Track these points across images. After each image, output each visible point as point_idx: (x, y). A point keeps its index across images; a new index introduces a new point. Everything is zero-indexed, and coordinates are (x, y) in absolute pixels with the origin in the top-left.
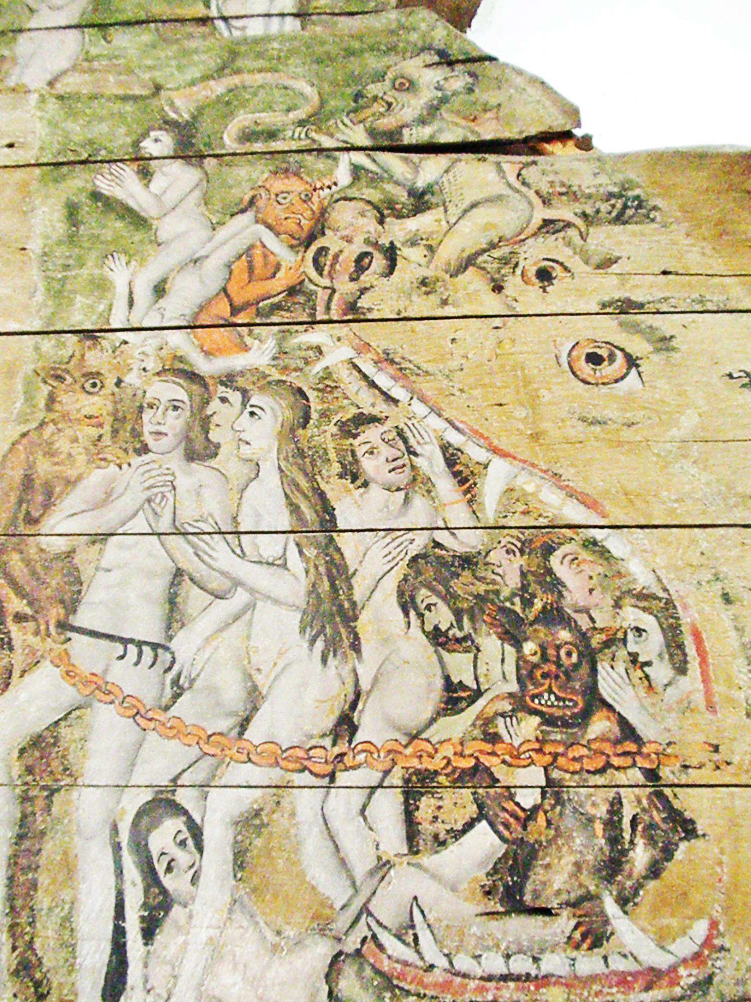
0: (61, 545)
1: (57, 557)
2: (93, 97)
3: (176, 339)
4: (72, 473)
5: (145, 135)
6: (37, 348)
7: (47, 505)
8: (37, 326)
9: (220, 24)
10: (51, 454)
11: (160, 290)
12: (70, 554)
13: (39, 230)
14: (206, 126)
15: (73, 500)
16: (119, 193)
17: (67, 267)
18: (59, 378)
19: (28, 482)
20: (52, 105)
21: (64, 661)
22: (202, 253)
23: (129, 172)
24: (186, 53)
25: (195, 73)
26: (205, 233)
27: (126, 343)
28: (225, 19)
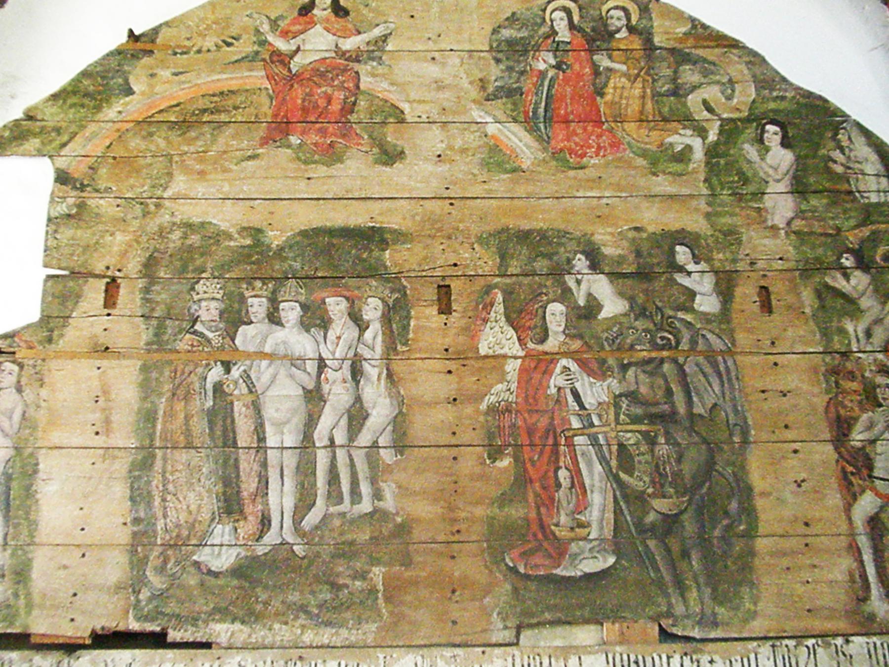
0: (859, 444)
1: (860, 449)
2: (811, 233)
3: (880, 356)
4: (854, 415)
5: (840, 257)
6: (824, 361)
7: (850, 428)
8: (821, 350)
9: (857, 194)
10: (845, 407)
11: (868, 334)
12: (864, 448)
13: (807, 303)
14: (867, 253)
15: (859, 427)
16: (837, 285)
17: (826, 322)
18: (838, 374)
19: (838, 418)
20: (793, 237)
21: (874, 489)
22: (882, 317)
23: (839, 275)
24: (845, 211)
25: (852, 222)
26: (880, 308)
27: (860, 358)
28: (859, 192)
